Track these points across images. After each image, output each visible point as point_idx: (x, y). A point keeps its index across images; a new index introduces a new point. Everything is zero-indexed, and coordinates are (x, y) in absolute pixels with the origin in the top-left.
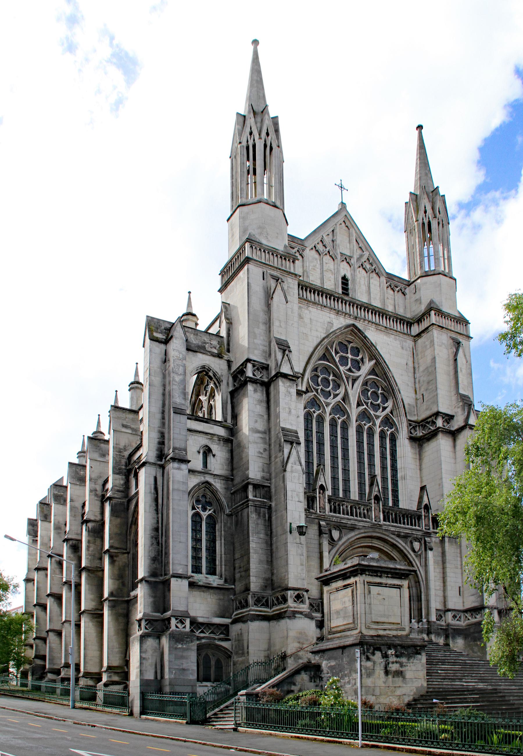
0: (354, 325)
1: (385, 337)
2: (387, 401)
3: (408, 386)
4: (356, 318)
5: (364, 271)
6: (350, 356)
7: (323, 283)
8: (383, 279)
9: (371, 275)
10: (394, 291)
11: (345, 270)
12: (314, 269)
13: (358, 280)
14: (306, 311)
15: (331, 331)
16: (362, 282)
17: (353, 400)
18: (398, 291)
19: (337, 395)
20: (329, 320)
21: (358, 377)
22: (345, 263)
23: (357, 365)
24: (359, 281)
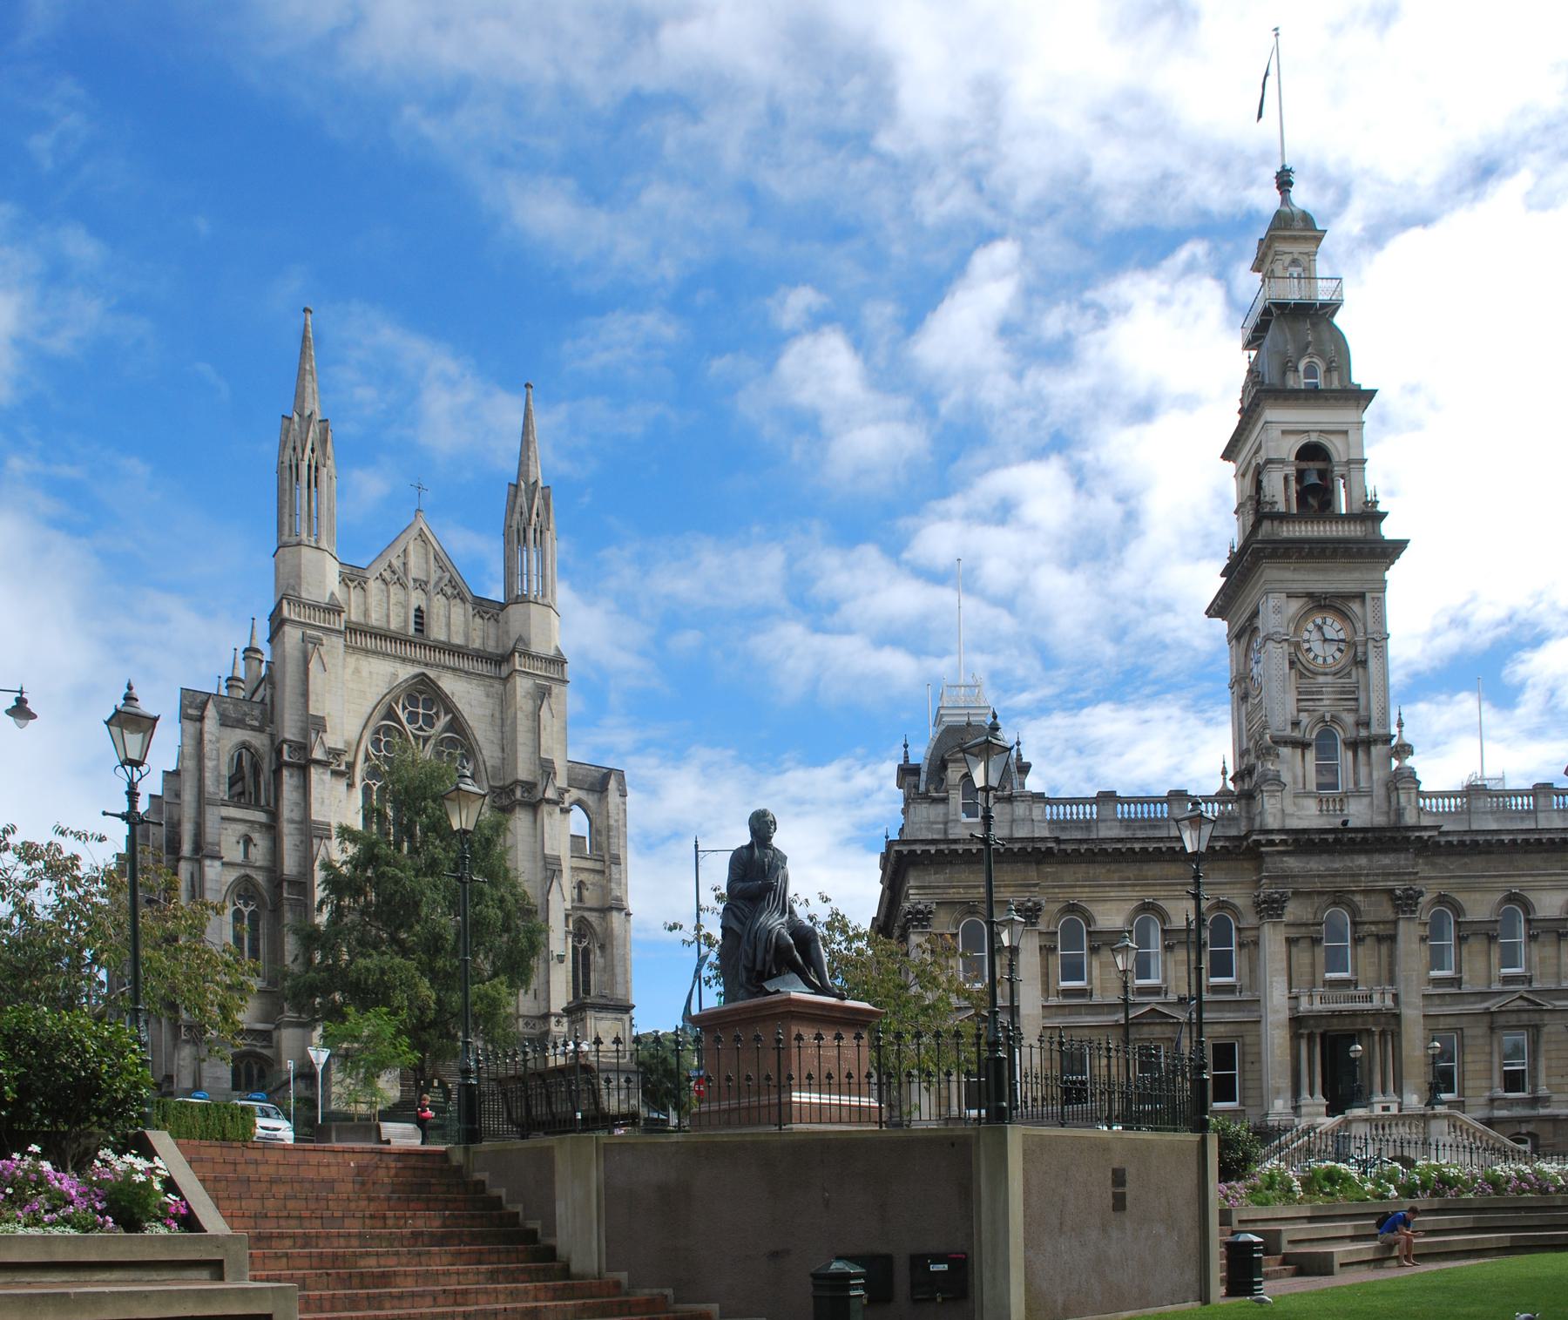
0: (424, 674)
4: (426, 665)
7: (388, 622)
9: (453, 602)
13: (435, 611)
14: (365, 663)
16: (442, 612)
20: (393, 670)
22: (419, 591)
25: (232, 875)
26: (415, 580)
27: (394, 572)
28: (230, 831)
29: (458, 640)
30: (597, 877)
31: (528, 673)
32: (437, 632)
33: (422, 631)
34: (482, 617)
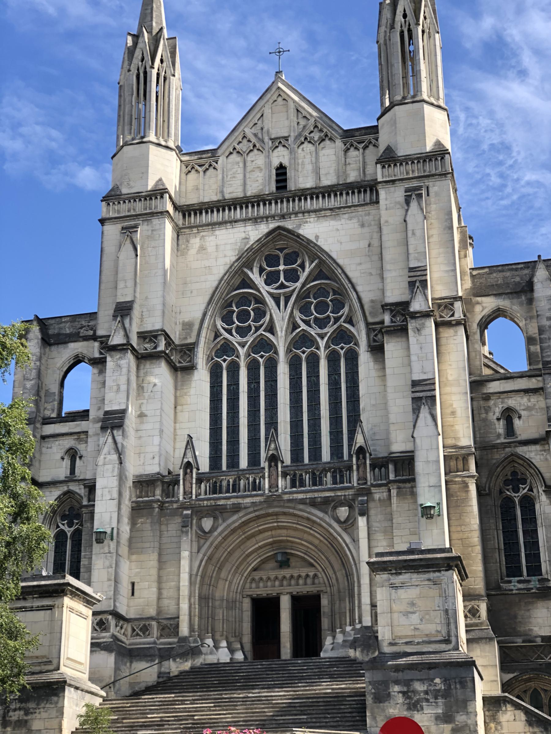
0: (279, 228)
2: (344, 307)
3: (371, 274)
5: (310, 145)
6: (282, 267)
7: (244, 190)
8: (339, 143)
10: (359, 150)
12: (234, 177)
13: (300, 161)
14: (212, 238)
15: (246, 249)
16: (308, 160)
17: (281, 326)
19: (261, 326)
20: (243, 235)
21: (294, 291)
22: (281, 148)
23: (292, 276)
24: (303, 162)
26: (273, 140)
28: (55, 449)
29: (328, 180)
31: (393, 181)
33: (285, 187)
34: (356, 148)
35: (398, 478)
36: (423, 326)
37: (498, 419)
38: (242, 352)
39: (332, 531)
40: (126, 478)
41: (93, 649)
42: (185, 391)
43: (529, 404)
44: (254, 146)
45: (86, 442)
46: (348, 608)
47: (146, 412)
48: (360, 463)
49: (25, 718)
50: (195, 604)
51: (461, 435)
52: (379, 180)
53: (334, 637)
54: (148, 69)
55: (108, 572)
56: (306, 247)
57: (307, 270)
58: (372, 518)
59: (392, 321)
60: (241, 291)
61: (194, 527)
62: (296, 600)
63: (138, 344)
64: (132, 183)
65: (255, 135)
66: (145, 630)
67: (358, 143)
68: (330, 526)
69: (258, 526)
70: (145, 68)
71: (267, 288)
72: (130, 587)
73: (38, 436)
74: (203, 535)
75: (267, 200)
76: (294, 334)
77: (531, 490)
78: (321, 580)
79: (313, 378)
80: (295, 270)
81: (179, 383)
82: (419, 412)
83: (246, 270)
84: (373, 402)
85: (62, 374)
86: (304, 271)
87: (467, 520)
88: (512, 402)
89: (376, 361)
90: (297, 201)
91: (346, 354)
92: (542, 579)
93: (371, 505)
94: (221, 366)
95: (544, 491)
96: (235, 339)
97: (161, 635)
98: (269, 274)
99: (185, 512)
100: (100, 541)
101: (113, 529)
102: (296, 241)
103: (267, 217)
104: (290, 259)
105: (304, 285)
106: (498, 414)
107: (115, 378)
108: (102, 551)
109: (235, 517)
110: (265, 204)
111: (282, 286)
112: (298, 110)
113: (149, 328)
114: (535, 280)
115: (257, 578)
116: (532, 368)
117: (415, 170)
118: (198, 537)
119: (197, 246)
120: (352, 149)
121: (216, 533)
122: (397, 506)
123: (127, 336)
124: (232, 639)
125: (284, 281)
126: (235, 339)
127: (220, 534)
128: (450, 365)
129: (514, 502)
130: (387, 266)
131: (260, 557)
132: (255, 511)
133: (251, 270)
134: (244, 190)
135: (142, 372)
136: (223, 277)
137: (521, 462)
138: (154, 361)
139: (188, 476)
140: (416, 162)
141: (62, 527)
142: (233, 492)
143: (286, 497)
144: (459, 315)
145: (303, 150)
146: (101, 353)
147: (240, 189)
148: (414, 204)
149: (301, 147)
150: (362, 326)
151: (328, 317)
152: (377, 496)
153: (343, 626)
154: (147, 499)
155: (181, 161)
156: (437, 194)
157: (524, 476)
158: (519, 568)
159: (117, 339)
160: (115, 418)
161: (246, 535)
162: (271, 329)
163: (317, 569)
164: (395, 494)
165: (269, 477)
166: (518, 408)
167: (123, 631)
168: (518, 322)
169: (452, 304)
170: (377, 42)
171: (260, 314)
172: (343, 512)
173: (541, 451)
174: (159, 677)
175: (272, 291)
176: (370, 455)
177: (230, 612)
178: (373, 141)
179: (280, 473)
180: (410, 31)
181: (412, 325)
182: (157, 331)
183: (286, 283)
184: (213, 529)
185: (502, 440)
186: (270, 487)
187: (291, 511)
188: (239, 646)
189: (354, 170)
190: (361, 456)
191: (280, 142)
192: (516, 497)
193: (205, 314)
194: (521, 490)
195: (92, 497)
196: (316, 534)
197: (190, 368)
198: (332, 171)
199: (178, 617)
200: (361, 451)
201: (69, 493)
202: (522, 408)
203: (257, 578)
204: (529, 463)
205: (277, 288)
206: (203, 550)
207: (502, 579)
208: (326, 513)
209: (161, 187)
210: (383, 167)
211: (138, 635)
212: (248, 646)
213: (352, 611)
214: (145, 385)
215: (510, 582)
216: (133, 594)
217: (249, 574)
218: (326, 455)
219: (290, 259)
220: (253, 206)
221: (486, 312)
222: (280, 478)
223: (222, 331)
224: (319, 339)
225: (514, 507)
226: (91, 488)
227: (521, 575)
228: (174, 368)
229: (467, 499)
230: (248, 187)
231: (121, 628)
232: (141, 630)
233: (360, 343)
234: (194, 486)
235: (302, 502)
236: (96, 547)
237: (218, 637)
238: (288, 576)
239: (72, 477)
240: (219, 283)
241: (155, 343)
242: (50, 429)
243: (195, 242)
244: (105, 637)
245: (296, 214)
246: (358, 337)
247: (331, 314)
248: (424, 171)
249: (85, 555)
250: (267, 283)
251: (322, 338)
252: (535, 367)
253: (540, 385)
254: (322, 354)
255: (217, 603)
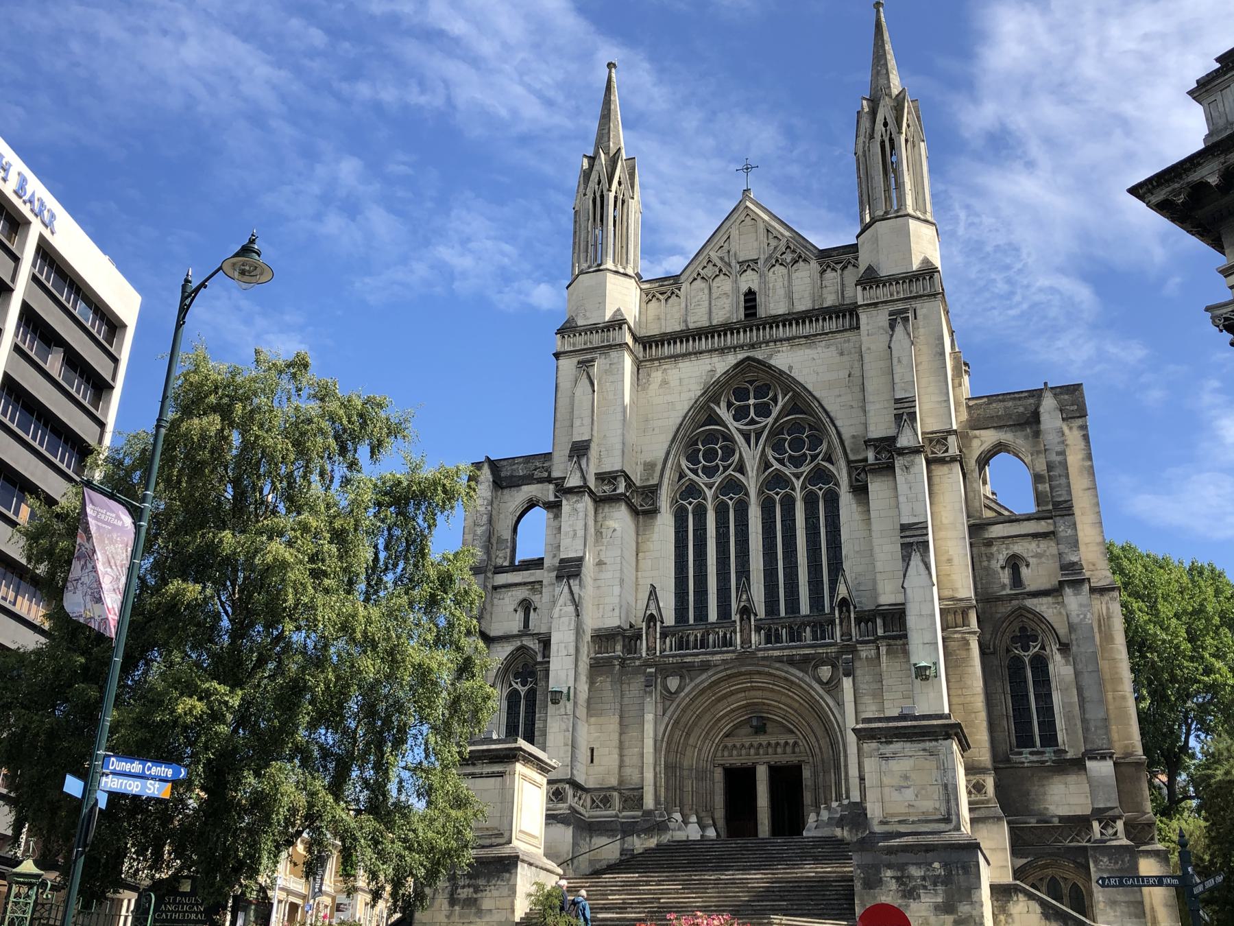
0: (748, 358)
1: (808, 351)
3: (852, 407)
6: (752, 401)
8: (814, 264)
11: (749, 281)
12: (699, 305)
13: (771, 285)
14: (675, 371)
16: (779, 284)
17: (752, 465)
18: (843, 269)
19: (730, 465)
20: (709, 368)
21: (765, 426)
22: (749, 272)
23: (763, 411)
25: (502, 653)
27: (714, 265)
28: (507, 600)
29: (802, 305)
30: (1044, 545)
31: (875, 305)
32: (772, 305)
33: (755, 314)
35: (887, 634)
36: (912, 463)
37: (1003, 568)
38: (709, 493)
39: (813, 693)
40: (584, 631)
41: (549, 821)
42: (648, 536)
43: (1039, 550)
44: (721, 270)
45: (541, 593)
46: (833, 781)
47: (605, 560)
48: (843, 616)
49: (475, 896)
50: (660, 773)
51: (958, 585)
52: (859, 304)
53: (818, 814)
54: (605, 192)
55: (565, 736)
56: (779, 379)
57: (780, 404)
58: (859, 679)
59: (876, 459)
60: (708, 428)
61: (659, 688)
62: (774, 771)
63: (596, 487)
64: (588, 314)
65: (722, 259)
66: (606, 801)
67: (836, 264)
68: (811, 687)
69: (730, 687)
70: (602, 192)
71: (736, 424)
72: (589, 754)
73: (490, 587)
74: (669, 696)
75: (735, 329)
76: (766, 473)
77: (1043, 648)
78: (802, 748)
79: (788, 522)
80: (767, 404)
81: (641, 529)
82: (910, 560)
83: (712, 405)
84: (857, 548)
85: (515, 519)
86: (776, 405)
87: (969, 683)
88: (1019, 548)
89: (859, 503)
90: (768, 329)
91: (825, 495)
92: (1059, 750)
93: (857, 664)
94: (687, 510)
95: (1058, 649)
96: (702, 480)
97: (624, 808)
98: (738, 409)
99: (648, 670)
100: (555, 702)
101: (569, 688)
102: (767, 372)
103: (735, 348)
104: (761, 392)
105: (776, 420)
106: (1002, 562)
107: (571, 522)
108: (558, 712)
109: (704, 676)
110: (732, 334)
111: (753, 422)
112: (768, 231)
113: (607, 468)
114: (1042, 410)
115: (729, 745)
116: (1040, 509)
117: (900, 291)
118: (664, 698)
119: (660, 379)
120: (829, 270)
121: (683, 694)
122: (887, 666)
123: (584, 478)
124: (703, 814)
125: (754, 417)
126: (702, 480)
127: (687, 695)
128: (945, 507)
129: (1024, 662)
130: (869, 398)
131: (732, 721)
132: (726, 669)
133: (718, 405)
134: (710, 319)
135: (600, 518)
136: (688, 413)
137: (1031, 616)
138: (614, 504)
139: (651, 630)
140: (901, 282)
141: (515, 685)
142: (701, 648)
143: (760, 654)
144: (953, 450)
145: (774, 273)
146: (556, 496)
147: (706, 317)
148: (899, 329)
149: (772, 270)
150: (842, 464)
151: (805, 454)
152: (863, 654)
153: (828, 802)
154: (607, 655)
155: (641, 289)
156: (925, 317)
157: (1034, 633)
158: (1032, 737)
159: (574, 481)
160: (571, 566)
161: (716, 696)
162: (741, 469)
163: (796, 735)
164: (884, 652)
165: (741, 631)
166: (1025, 555)
167: (582, 801)
168: (1023, 457)
169: (946, 439)
170: (855, 154)
171: (729, 452)
172: (825, 672)
173: (1053, 603)
174: (621, 855)
175: (741, 427)
176: (855, 607)
177: (700, 783)
178: (853, 261)
179: (753, 627)
180: (891, 140)
181: (899, 462)
182: (617, 472)
183: (757, 419)
184: (680, 689)
185: (1008, 591)
186: (742, 642)
187: (767, 669)
188: (711, 822)
189: (831, 293)
190: (844, 609)
191: (749, 265)
192: (1027, 656)
193: (668, 454)
194: (1031, 648)
195: (546, 653)
196: (795, 697)
197: (653, 512)
198: (807, 294)
199: (643, 788)
200: (844, 603)
201: (522, 648)
202: (1031, 554)
203: (729, 745)
204: (1040, 618)
205: (746, 424)
206: (669, 713)
207: (1011, 750)
208: (807, 673)
209: (619, 318)
210: (864, 289)
211: (598, 806)
212: (721, 823)
213: (838, 785)
214: (603, 530)
215: (1021, 753)
216: (592, 761)
217: (721, 740)
218: (805, 608)
219: (761, 392)
220: (719, 336)
221: (986, 446)
222: (753, 633)
223: (688, 471)
224: (794, 479)
225: (1024, 668)
226: (546, 643)
227: (1034, 746)
228: (635, 512)
229: (967, 659)
230: (714, 315)
231: (580, 799)
232: (601, 802)
233: (841, 483)
234: (658, 641)
235: (779, 659)
236: (551, 708)
237: (686, 811)
238: (764, 743)
239: (525, 631)
240: (683, 420)
241: (614, 485)
242: (501, 579)
243: (657, 376)
244: (562, 808)
245: (767, 343)
246: (838, 477)
247: (807, 452)
248: (911, 292)
249: (540, 717)
250: (736, 419)
251: (798, 478)
252: (1044, 508)
253: (1051, 528)
254: (798, 495)
255: (685, 773)
